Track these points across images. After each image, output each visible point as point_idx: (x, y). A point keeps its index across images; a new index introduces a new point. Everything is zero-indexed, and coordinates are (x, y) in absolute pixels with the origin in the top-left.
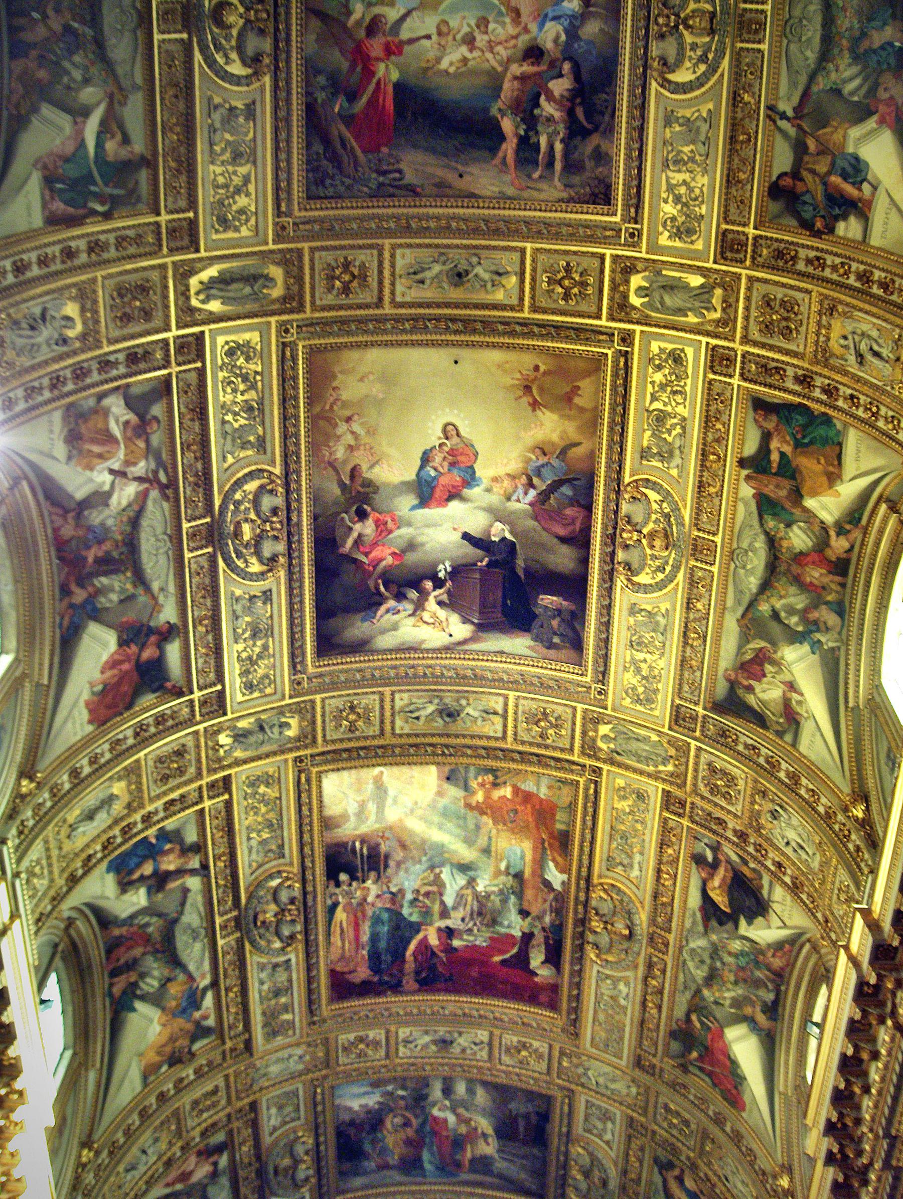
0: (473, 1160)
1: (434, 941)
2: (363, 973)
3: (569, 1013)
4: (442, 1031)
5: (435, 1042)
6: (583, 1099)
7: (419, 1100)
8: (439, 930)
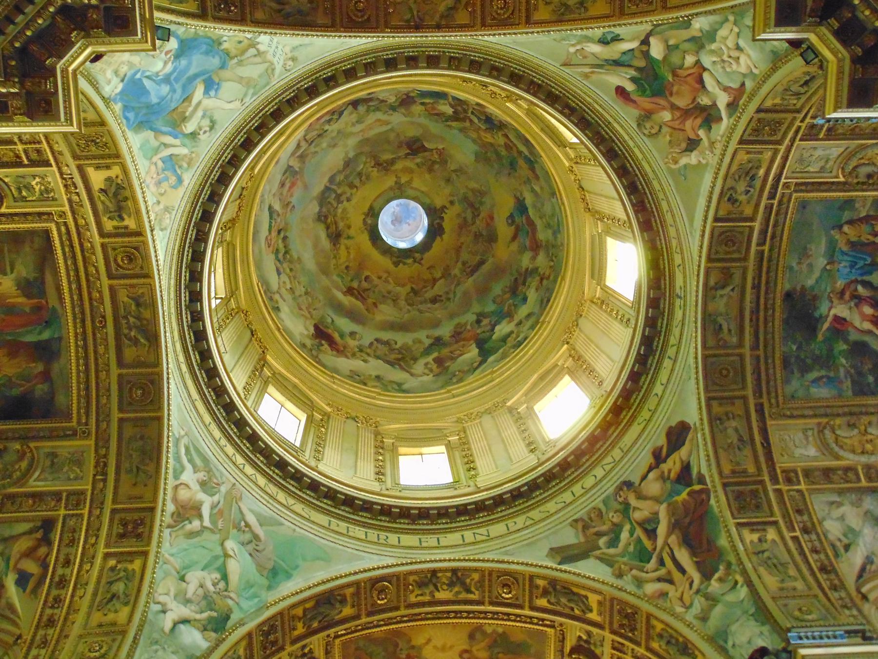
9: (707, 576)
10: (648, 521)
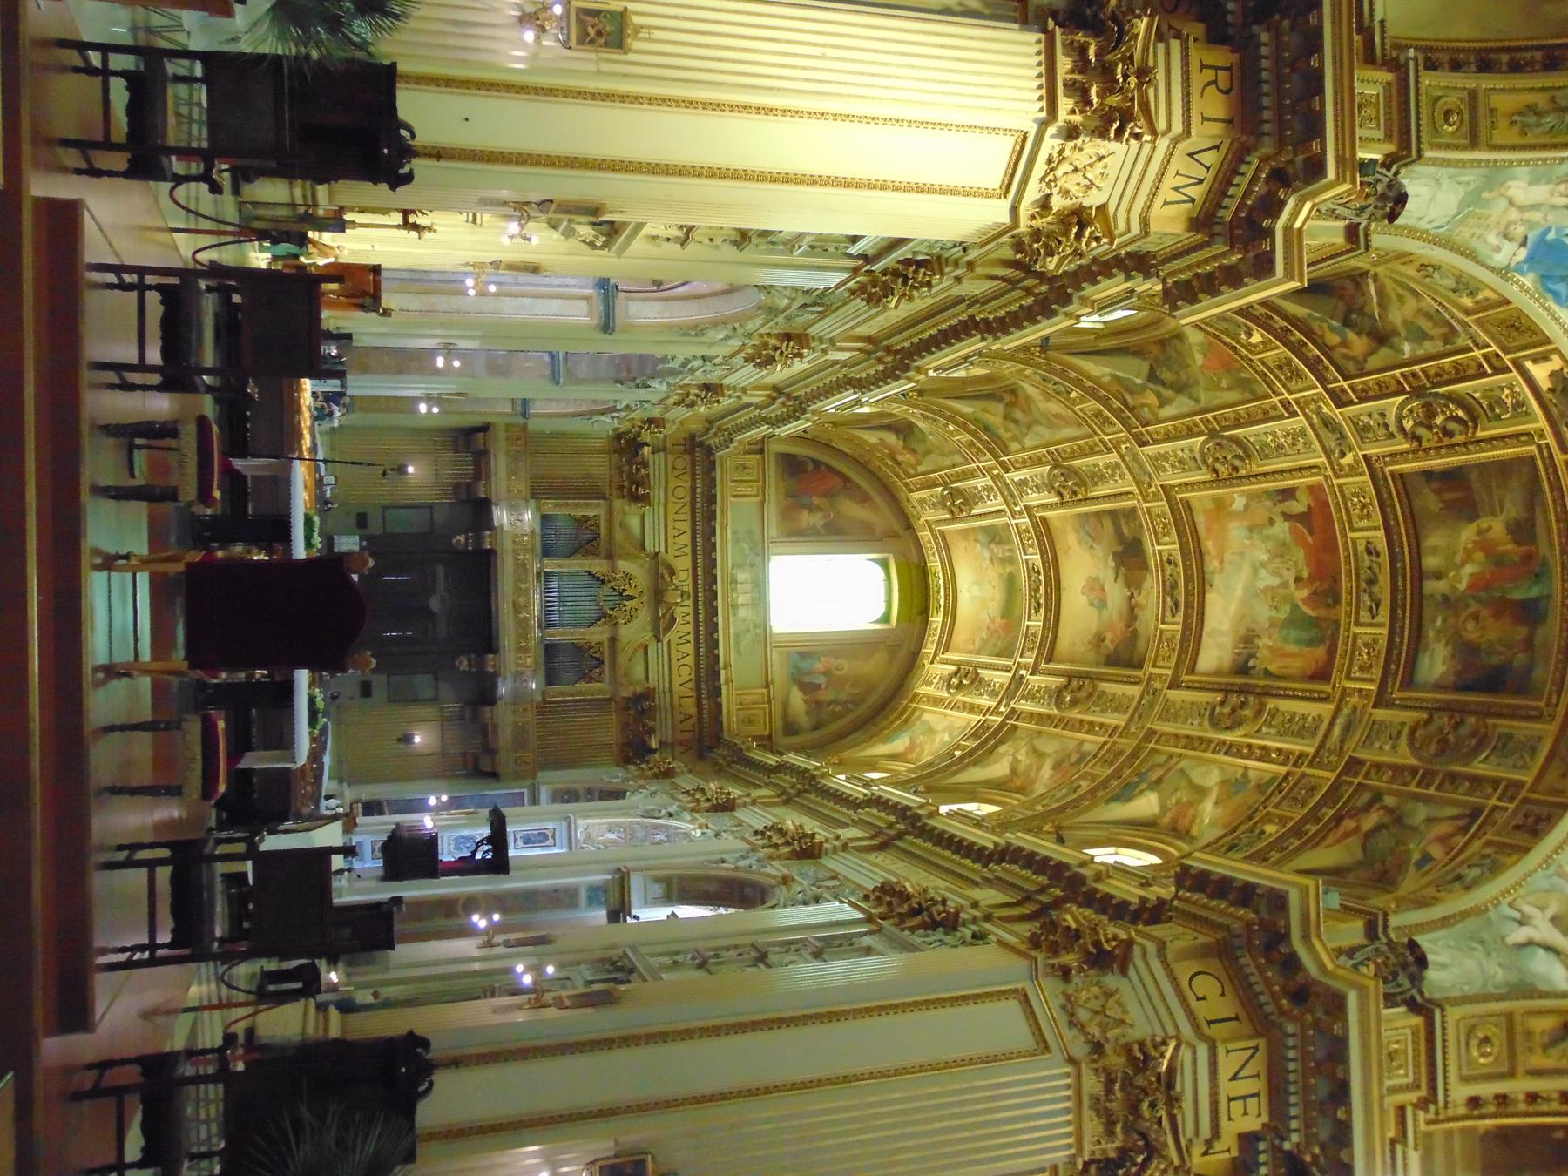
0: (1518, 542)
1: (1304, 593)
2: (1320, 652)
8: (1297, 588)
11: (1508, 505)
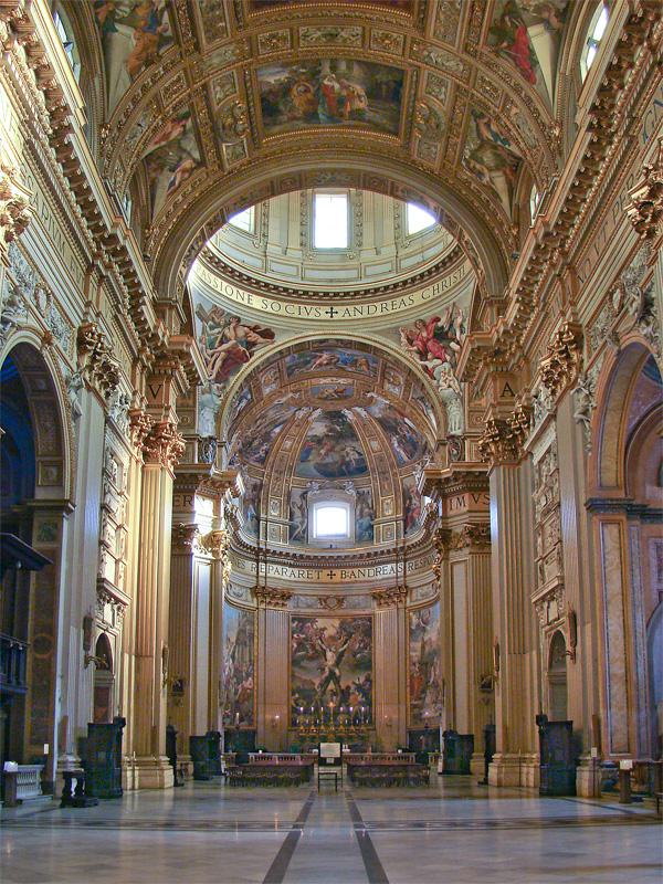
0: (350, 112)
3: (419, 14)
4: (330, 29)
5: (325, 36)
6: (426, 72)
7: (315, 74)
9: (217, 380)
10: (226, 338)
11: (372, 114)
